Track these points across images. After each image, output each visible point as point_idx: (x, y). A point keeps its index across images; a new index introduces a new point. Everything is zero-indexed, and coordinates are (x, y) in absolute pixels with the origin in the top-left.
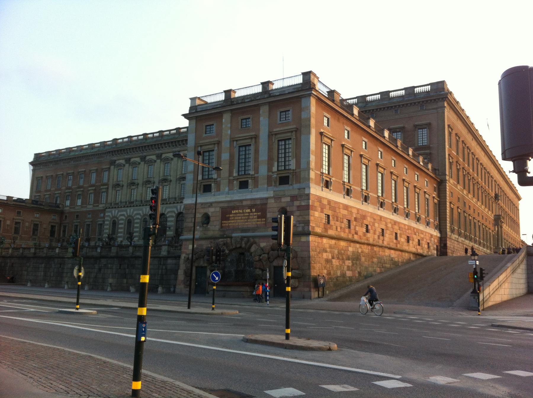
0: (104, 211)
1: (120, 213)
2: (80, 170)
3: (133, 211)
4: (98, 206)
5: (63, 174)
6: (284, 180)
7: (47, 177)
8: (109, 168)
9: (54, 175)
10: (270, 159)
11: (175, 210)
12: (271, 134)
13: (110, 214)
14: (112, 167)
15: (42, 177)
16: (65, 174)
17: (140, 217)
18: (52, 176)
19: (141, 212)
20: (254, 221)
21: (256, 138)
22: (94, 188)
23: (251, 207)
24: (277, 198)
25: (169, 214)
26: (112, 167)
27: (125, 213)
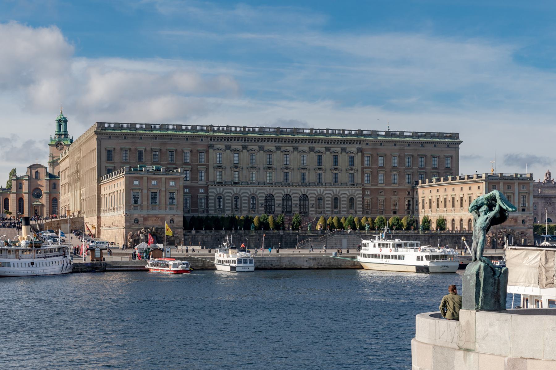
0: (206, 188)
1: (225, 191)
2: (168, 148)
3: (240, 191)
4: (197, 183)
5: (145, 149)
6: (523, 210)
7: (121, 149)
8: (207, 152)
9: (132, 148)
10: (519, 202)
11: (282, 192)
12: (519, 193)
13: (214, 191)
14: (211, 151)
15: (114, 149)
16: (148, 149)
17: (248, 195)
18: (130, 149)
19: (248, 191)
20: (513, 223)
21: (514, 194)
22: (190, 166)
23: (512, 218)
24: (522, 216)
25: (277, 195)
26: (211, 151)
27: (231, 191)
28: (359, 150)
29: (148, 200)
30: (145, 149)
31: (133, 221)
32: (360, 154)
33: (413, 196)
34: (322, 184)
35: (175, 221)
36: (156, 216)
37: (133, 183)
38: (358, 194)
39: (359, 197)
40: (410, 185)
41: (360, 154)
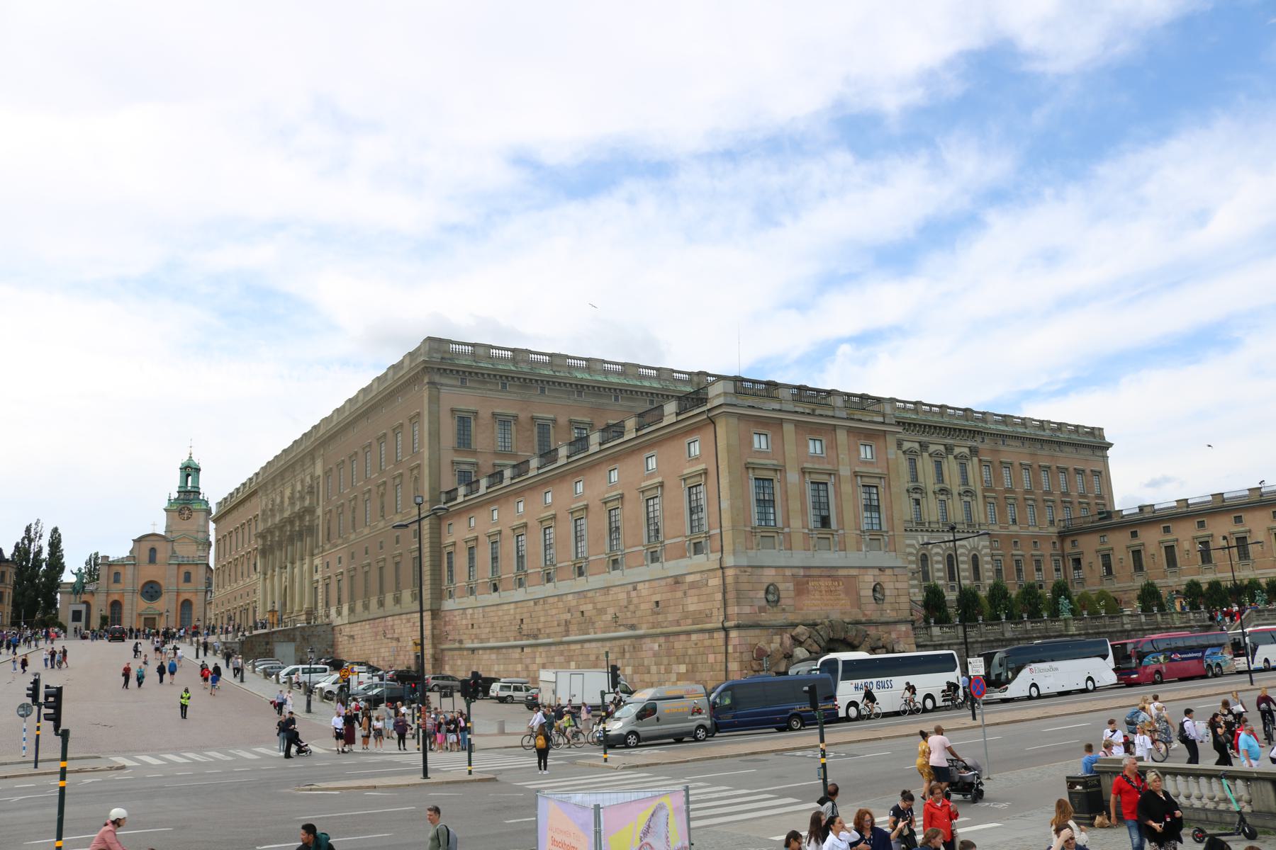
9: (523, 416)
18: (516, 417)
28: (974, 452)
29: (804, 511)
30: (554, 421)
31: (762, 594)
32: (975, 459)
33: (1063, 550)
34: (923, 524)
35: (887, 592)
36: (830, 573)
37: (751, 443)
38: (985, 547)
39: (986, 555)
40: (1054, 530)
41: (975, 459)
